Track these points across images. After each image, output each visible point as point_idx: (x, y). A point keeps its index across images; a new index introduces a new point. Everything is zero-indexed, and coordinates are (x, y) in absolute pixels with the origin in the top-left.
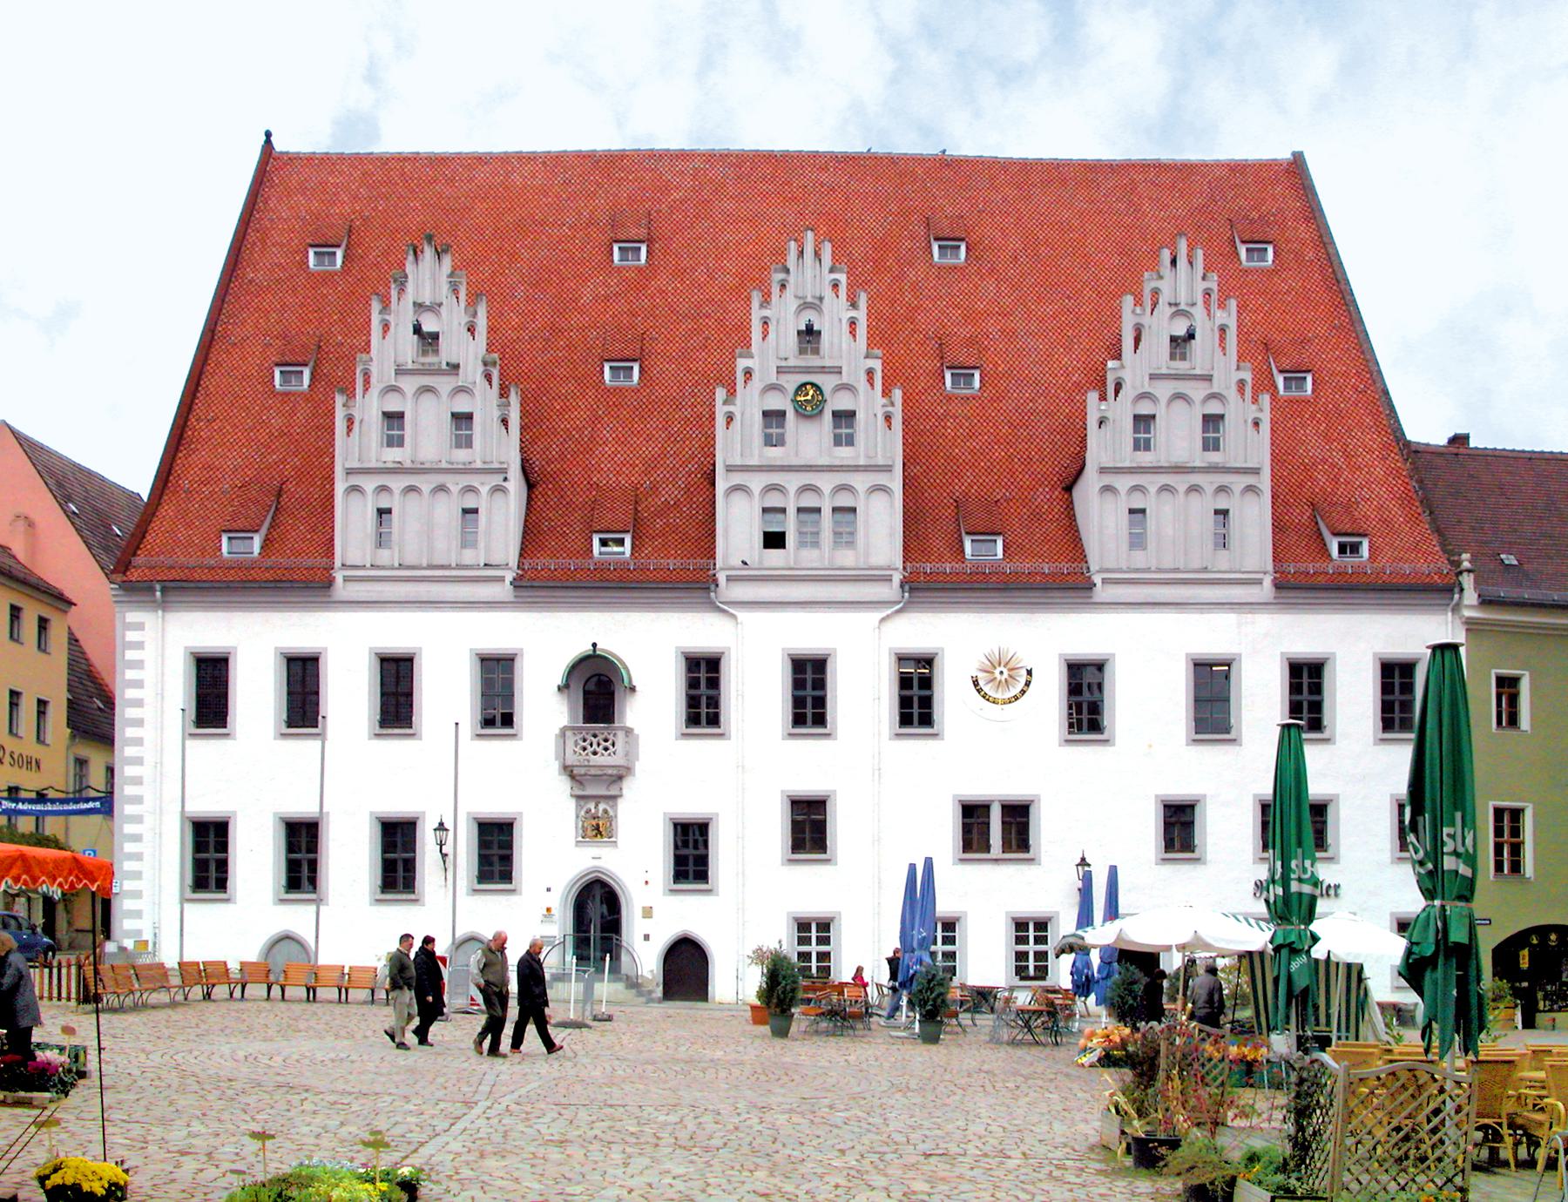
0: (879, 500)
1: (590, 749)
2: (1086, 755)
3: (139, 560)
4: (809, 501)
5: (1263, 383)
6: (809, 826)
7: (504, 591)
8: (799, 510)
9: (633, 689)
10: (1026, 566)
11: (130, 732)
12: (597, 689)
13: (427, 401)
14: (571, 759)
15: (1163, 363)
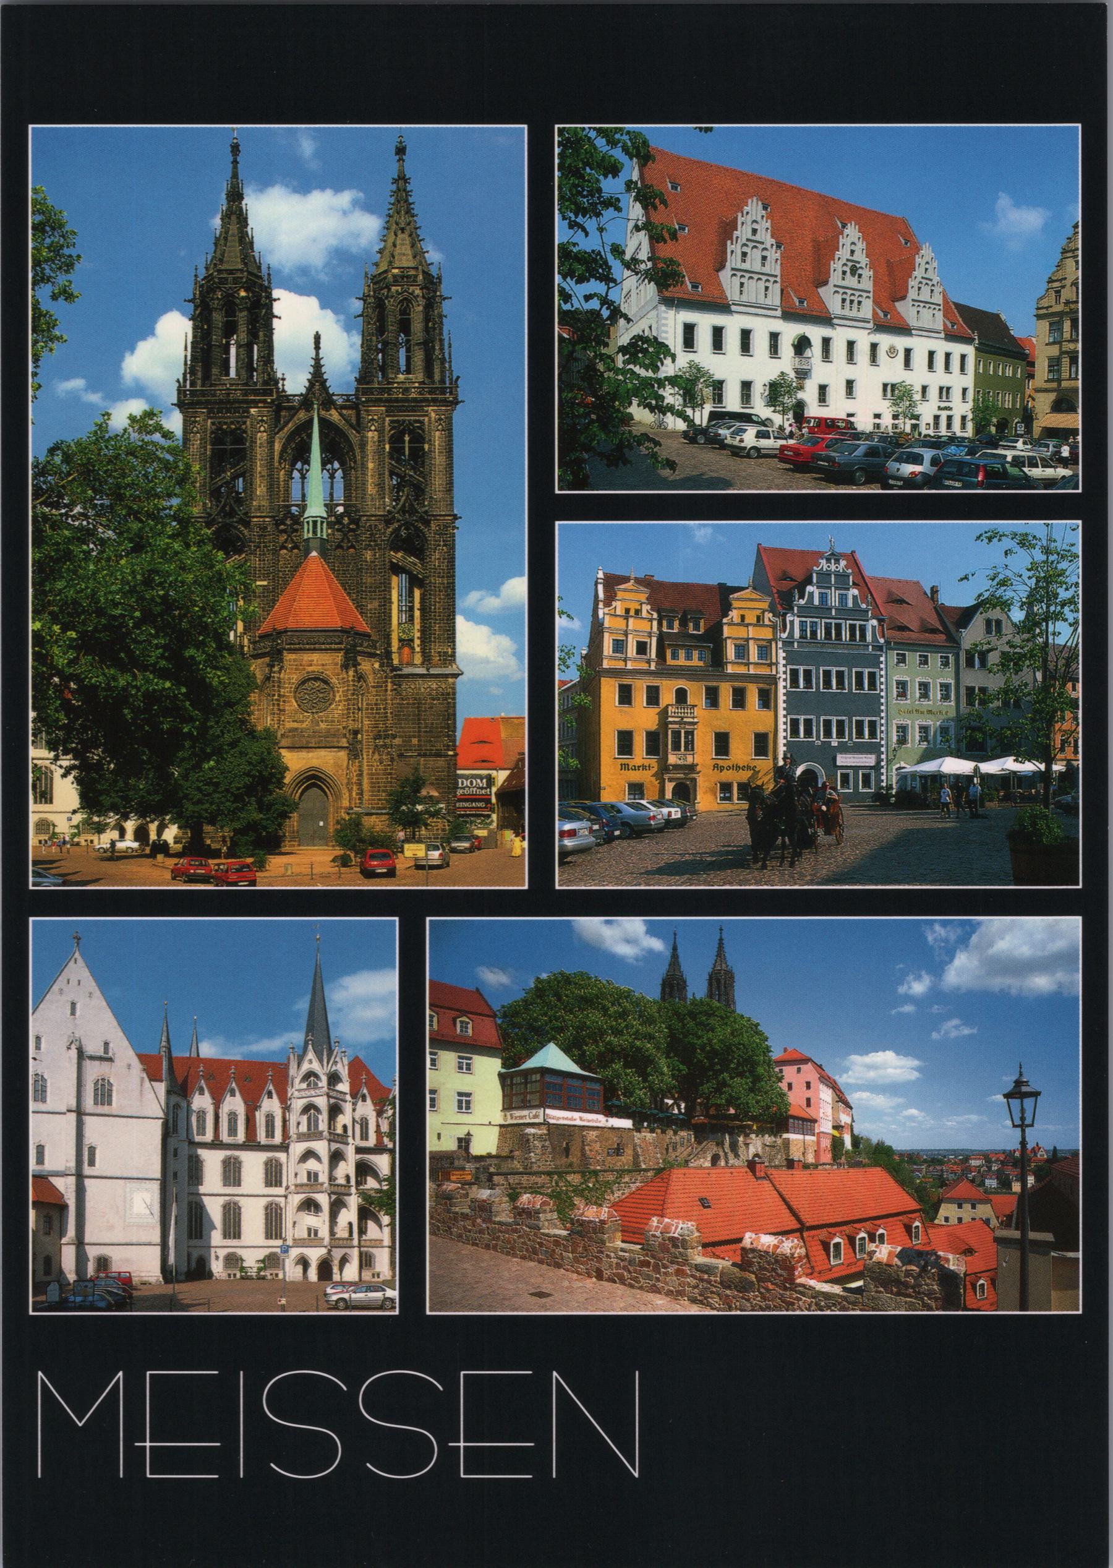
6: (850, 384)
7: (779, 313)
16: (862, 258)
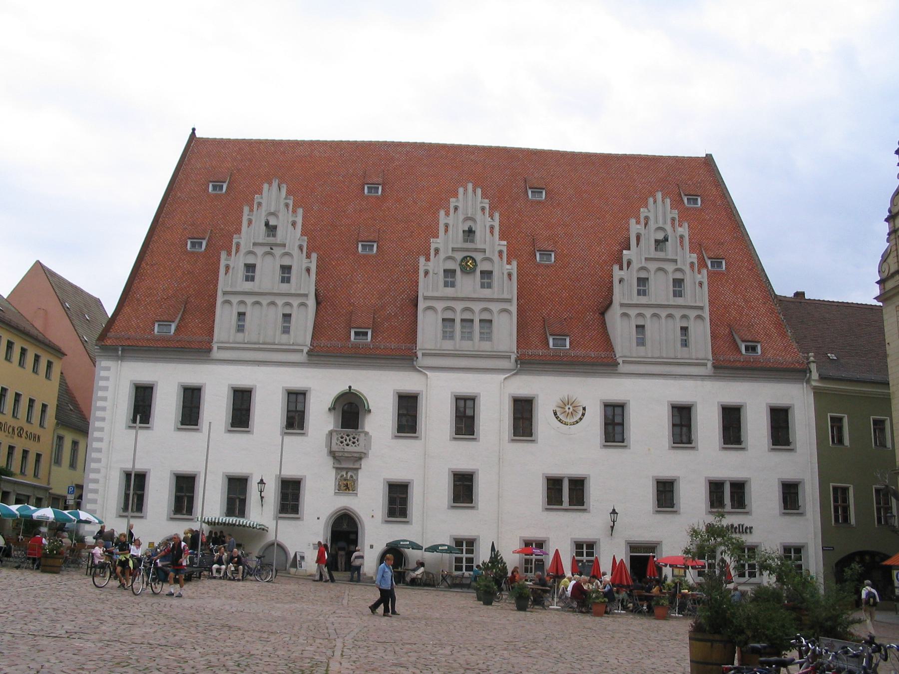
0: (505, 316)
1: (345, 443)
2: (614, 454)
3: (109, 335)
4: (467, 316)
5: (702, 264)
6: (463, 488)
8: (462, 320)
9: (370, 411)
10: (581, 352)
11: (98, 424)
12: (350, 411)
13: (269, 259)
14: (335, 448)
15: (653, 254)
16: (491, 243)
